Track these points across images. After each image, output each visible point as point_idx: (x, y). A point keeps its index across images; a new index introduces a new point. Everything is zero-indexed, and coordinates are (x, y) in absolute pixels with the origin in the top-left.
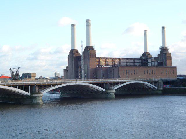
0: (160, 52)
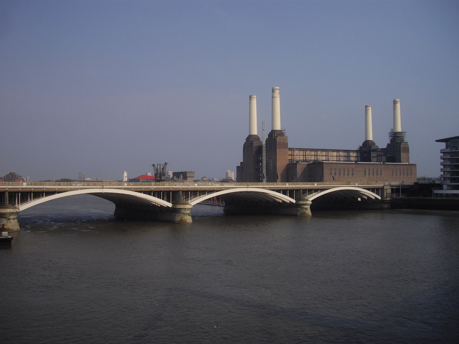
0: (391, 141)
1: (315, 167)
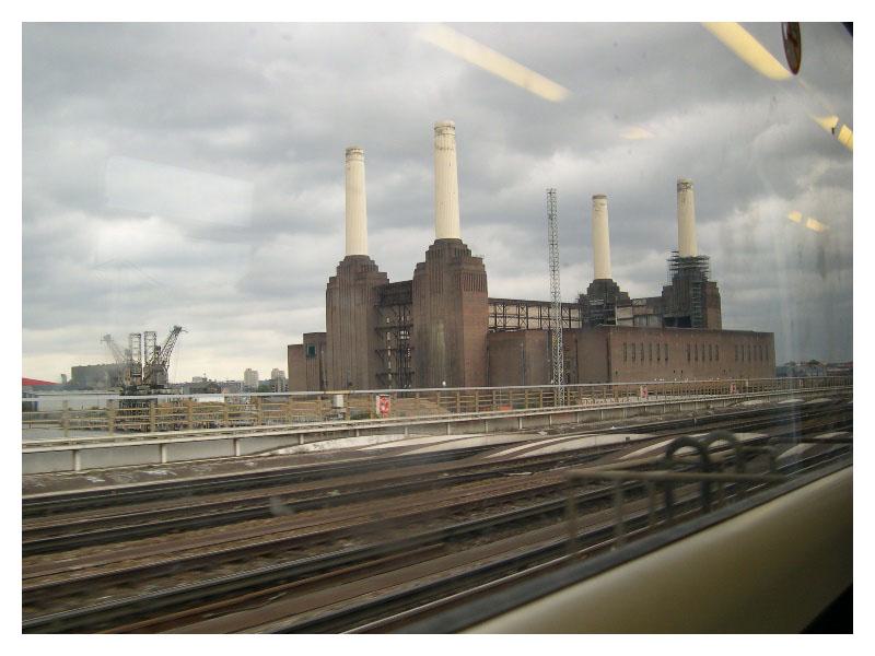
0: (675, 279)
1: (576, 341)
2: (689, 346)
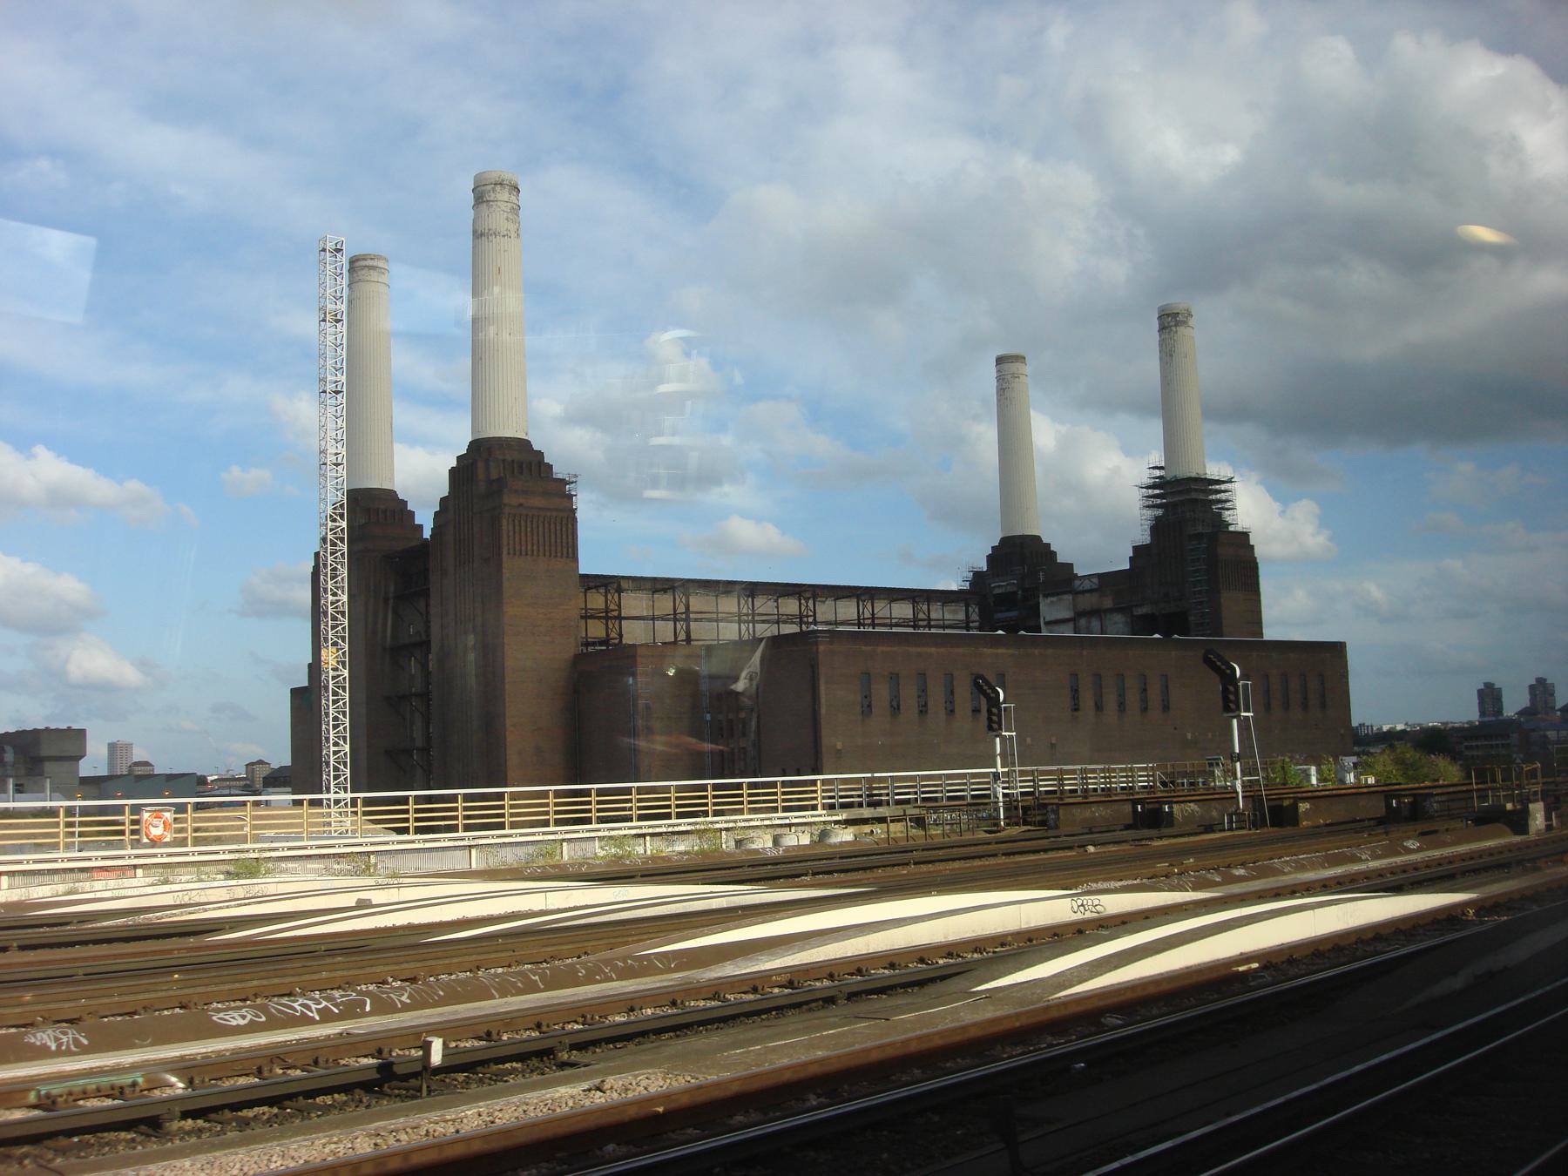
0: (1157, 528)
2: (1075, 675)
